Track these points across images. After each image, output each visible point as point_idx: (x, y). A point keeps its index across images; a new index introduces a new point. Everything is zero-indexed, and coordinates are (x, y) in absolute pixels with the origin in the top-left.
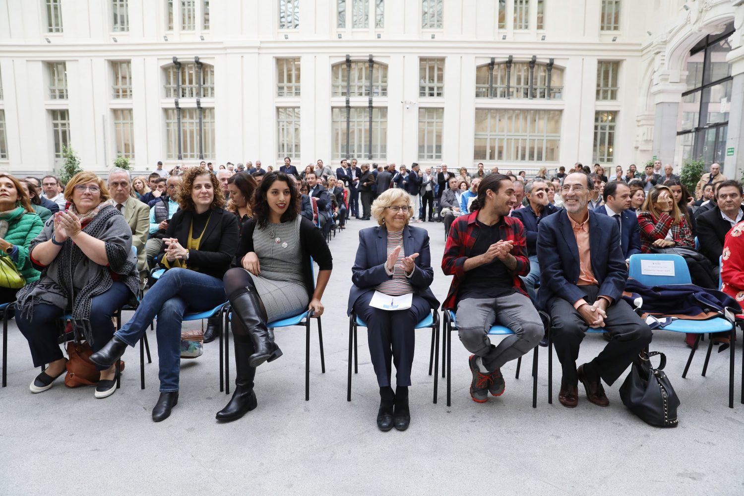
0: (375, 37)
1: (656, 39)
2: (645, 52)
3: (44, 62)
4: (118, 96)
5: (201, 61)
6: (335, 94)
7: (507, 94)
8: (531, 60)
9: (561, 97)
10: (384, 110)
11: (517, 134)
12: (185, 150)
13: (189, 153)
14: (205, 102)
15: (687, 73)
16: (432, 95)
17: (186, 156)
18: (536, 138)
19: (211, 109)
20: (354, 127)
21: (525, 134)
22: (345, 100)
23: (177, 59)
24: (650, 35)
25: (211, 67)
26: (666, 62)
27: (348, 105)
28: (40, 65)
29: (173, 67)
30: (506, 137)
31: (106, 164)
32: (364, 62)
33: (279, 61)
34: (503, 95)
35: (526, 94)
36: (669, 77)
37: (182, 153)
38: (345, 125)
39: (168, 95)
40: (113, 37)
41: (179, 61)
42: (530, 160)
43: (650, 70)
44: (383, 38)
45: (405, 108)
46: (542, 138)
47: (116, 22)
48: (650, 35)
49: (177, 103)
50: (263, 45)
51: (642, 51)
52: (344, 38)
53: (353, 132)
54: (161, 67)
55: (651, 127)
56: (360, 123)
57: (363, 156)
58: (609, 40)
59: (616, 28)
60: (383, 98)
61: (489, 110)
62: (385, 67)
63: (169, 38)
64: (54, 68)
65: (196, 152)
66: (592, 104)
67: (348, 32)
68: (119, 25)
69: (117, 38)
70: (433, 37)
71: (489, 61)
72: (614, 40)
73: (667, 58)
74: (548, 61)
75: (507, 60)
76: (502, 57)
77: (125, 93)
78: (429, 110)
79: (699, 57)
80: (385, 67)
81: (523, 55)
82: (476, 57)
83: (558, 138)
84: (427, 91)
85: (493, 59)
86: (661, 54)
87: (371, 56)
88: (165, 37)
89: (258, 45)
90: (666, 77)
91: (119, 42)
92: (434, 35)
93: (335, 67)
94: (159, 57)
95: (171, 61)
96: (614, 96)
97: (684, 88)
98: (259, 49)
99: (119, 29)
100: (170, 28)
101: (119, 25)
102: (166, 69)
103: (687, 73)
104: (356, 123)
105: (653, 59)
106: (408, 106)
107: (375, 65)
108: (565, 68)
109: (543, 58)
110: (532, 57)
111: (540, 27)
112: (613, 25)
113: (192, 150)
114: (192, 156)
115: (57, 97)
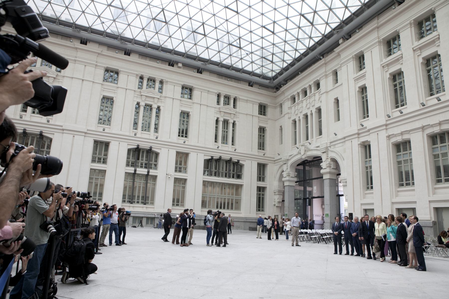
1: (284, 156)
2: (276, 162)
6: (128, 165)
8: (229, 159)
10: (155, 177)
11: (221, 195)
15: (296, 173)
18: (212, 196)
20: (137, 184)
21: (215, 195)
22: (134, 169)
24: (279, 155)
26: (289, 168)
30: (227, 198)
34: (215, 175)
35: (226, 176)
36: (291, 175)
38: (131, 184)
43: (280, 171)
44: (159, 139)
45: (167, 178)
46: (215, 197)
48: (279, 155)
50: (88, 132)
51: (275, 161)
53: (136, 187)
55: (280, 196)
56: (140, 183)
58: (262, 155)
59: (263, 149)
61: (216, 183)
62: (157, 154)
66: (256, 184)
72: (264, 155)
73: (289, 166)
78: (180, 180)
79: (301, 167)
81: (226, 157)
83: (240, 199)
84: (178, 169)
85: (212, 157)
86: (287, 164)
87: (151, 147)
89: (86, 131)
90: (289, 174)
92: (185, 141)
93: (129, 150)
96: (263, 180)
97: (296, 179)
98: (85, 133)
103: (296, 173)
105: (282, 166)
106: (169, 177)
108: (244, 165)
109: (235, 159)
110: (230, 158)
111: (233, 144)
112: (262, 148)
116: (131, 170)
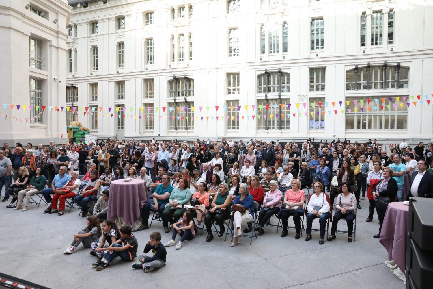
0: (282, 59)
3: (115, 81)
4: (147, 97)
5: (187, 77)
7: (369, 87)
9: (407, 87)
12: (179, 125)
13: (180, 126)
14: (189, 99)
16: (317, 90)
17: (179, 128)
19: (192, 103)
23: (175, 76)
25: (193, 80)
27: (266, 98)
28: (114, 82)
29: (174, 80)
31: (140, 131)
32: (276, 73)
33: (229, 75)
37: (177, 126)
39: (171, 96)
40: (146, 67)
41: (176, 77)
42: (385, 129)
47: (148, 60)
49: (175, 100)
52: (263, 60)
54: (168, 81)
57: (276, 128)
60: (288, 93)
62: (288, 75)
63: (172, 66)
64: (120, 84)
65: (184, 126)
67: (266, 57)
68: (149, 61)
69: (148, 68)
70: (317, 55)
71: (354, 67)
74: (396, 64)
75: (367, 65)
76: (362, 63)
77: (151, 96)
80: (288, 75)
82: (345, 66)
85: (357, 66)
88: (170, 66)
91: (149, 70)
94: (167, 76)
95: (172, 78)
99: (149, 63)
100: (174, 61)
101: (149, 61)
102: (170, 82)
104: (271, 108)
107: (283, 74)
113: (182, 125)
114: (182, 128)
115: (120, 98)
116: (262, 96)
